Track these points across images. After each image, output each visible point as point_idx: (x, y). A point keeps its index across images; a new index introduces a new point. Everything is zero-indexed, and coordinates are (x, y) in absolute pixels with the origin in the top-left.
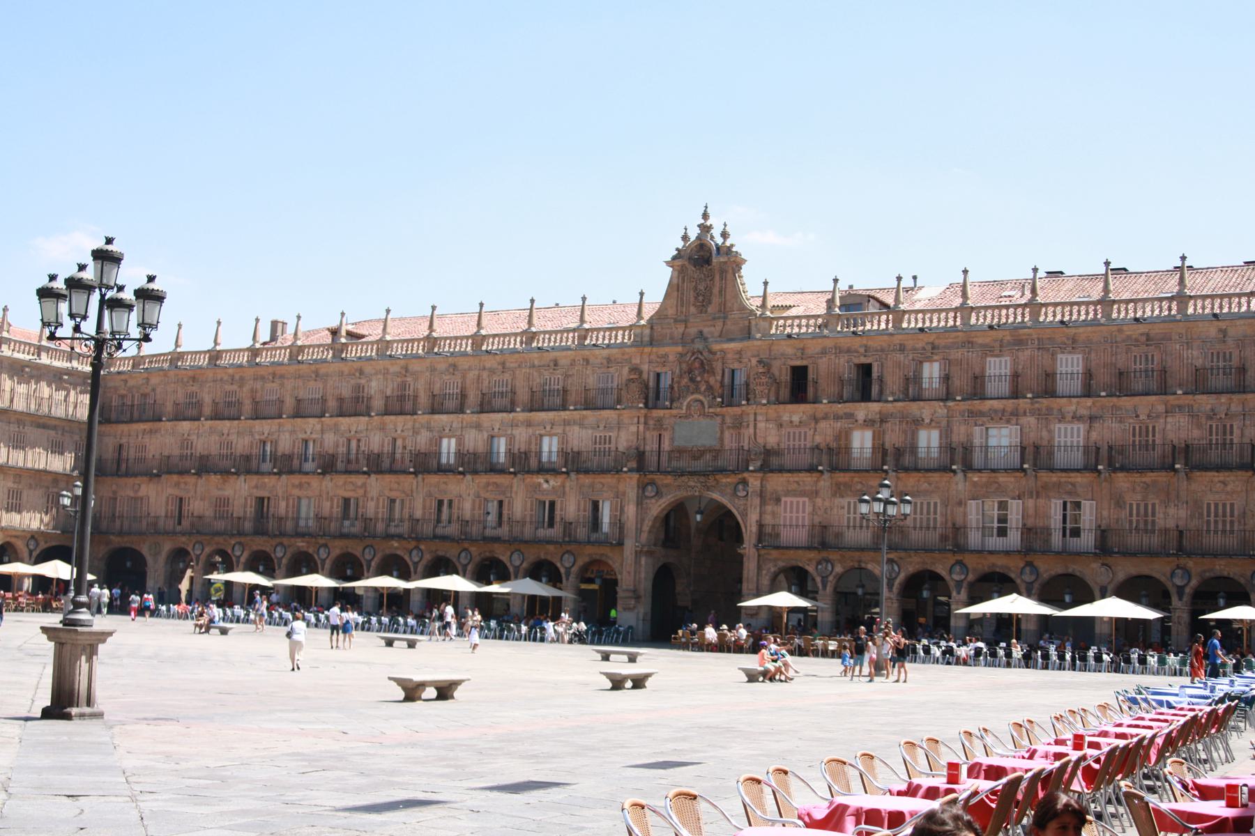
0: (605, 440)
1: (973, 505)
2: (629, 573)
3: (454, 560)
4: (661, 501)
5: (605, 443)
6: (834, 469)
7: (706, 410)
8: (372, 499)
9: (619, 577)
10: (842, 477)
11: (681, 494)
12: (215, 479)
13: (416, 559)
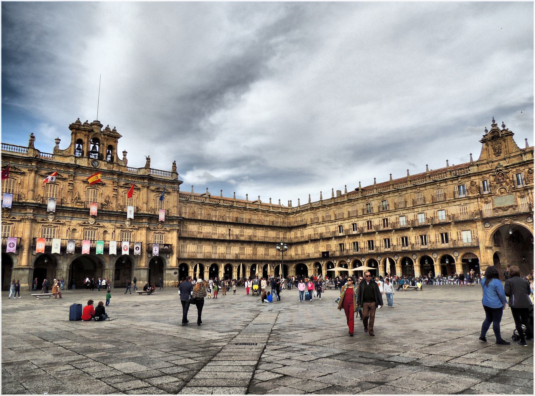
0: (464, 209)
2: (483, 256)
3: (411, 258)
4: (493, 228)
5: (465, 210)
7: (508, 192)
8: (378, 240)
9: (479, 258)
13: (396, 259)
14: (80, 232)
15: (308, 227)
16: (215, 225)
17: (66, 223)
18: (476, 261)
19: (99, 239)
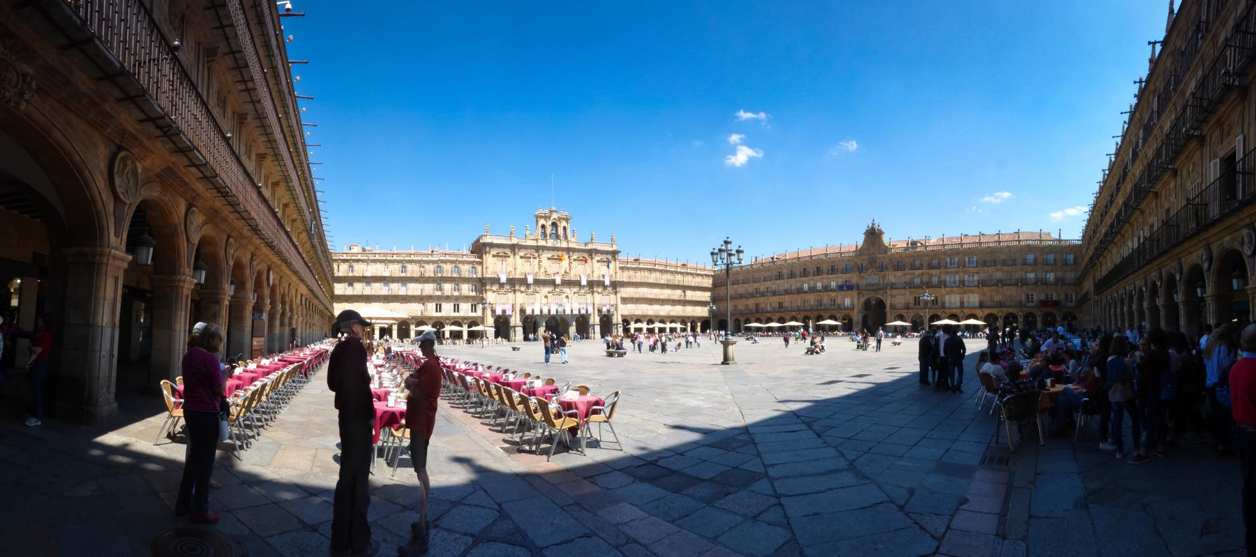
1: (947, 296)
6: (910, 288)
10: (912, 290)
11: (869, 296)
12: (744, 299)
18: (851, 321)
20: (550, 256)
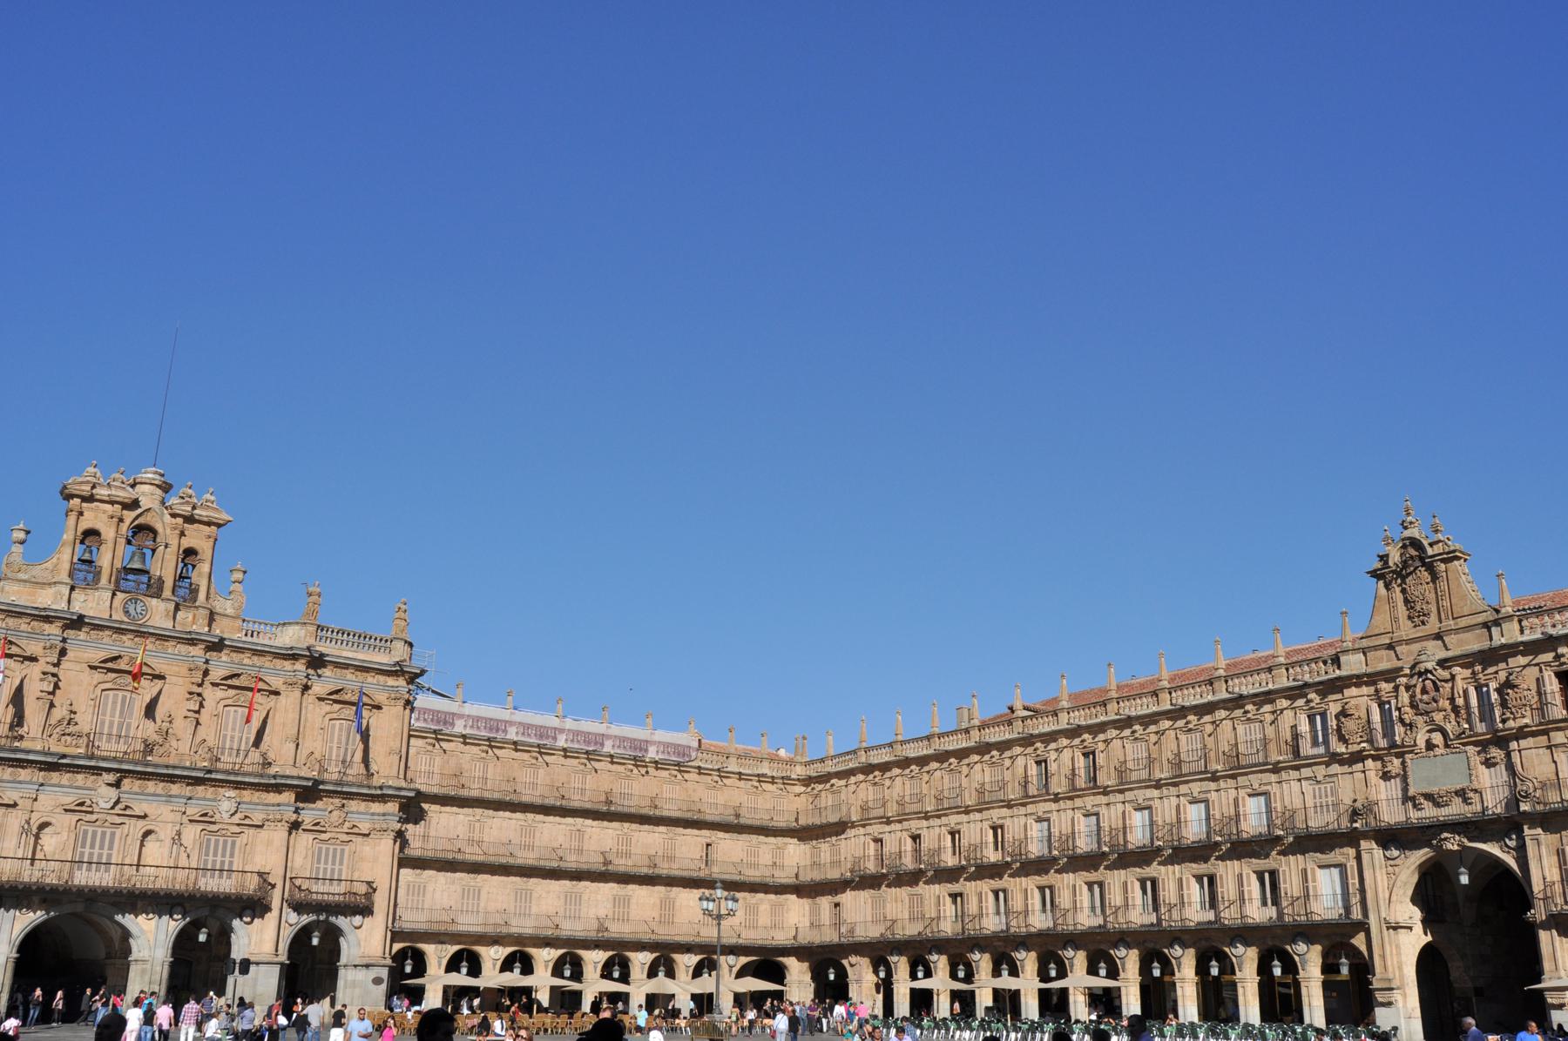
0: (1326, 791)
5: (1326, 796)
14: (65, 834)
15: (851, 833)
16: (530, 816)
17: (20, 802)
19: (124, 857)
20: (97, 656)
